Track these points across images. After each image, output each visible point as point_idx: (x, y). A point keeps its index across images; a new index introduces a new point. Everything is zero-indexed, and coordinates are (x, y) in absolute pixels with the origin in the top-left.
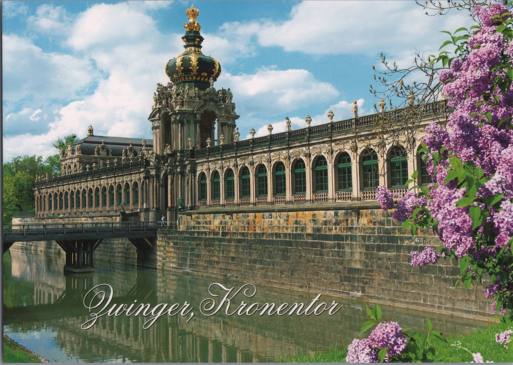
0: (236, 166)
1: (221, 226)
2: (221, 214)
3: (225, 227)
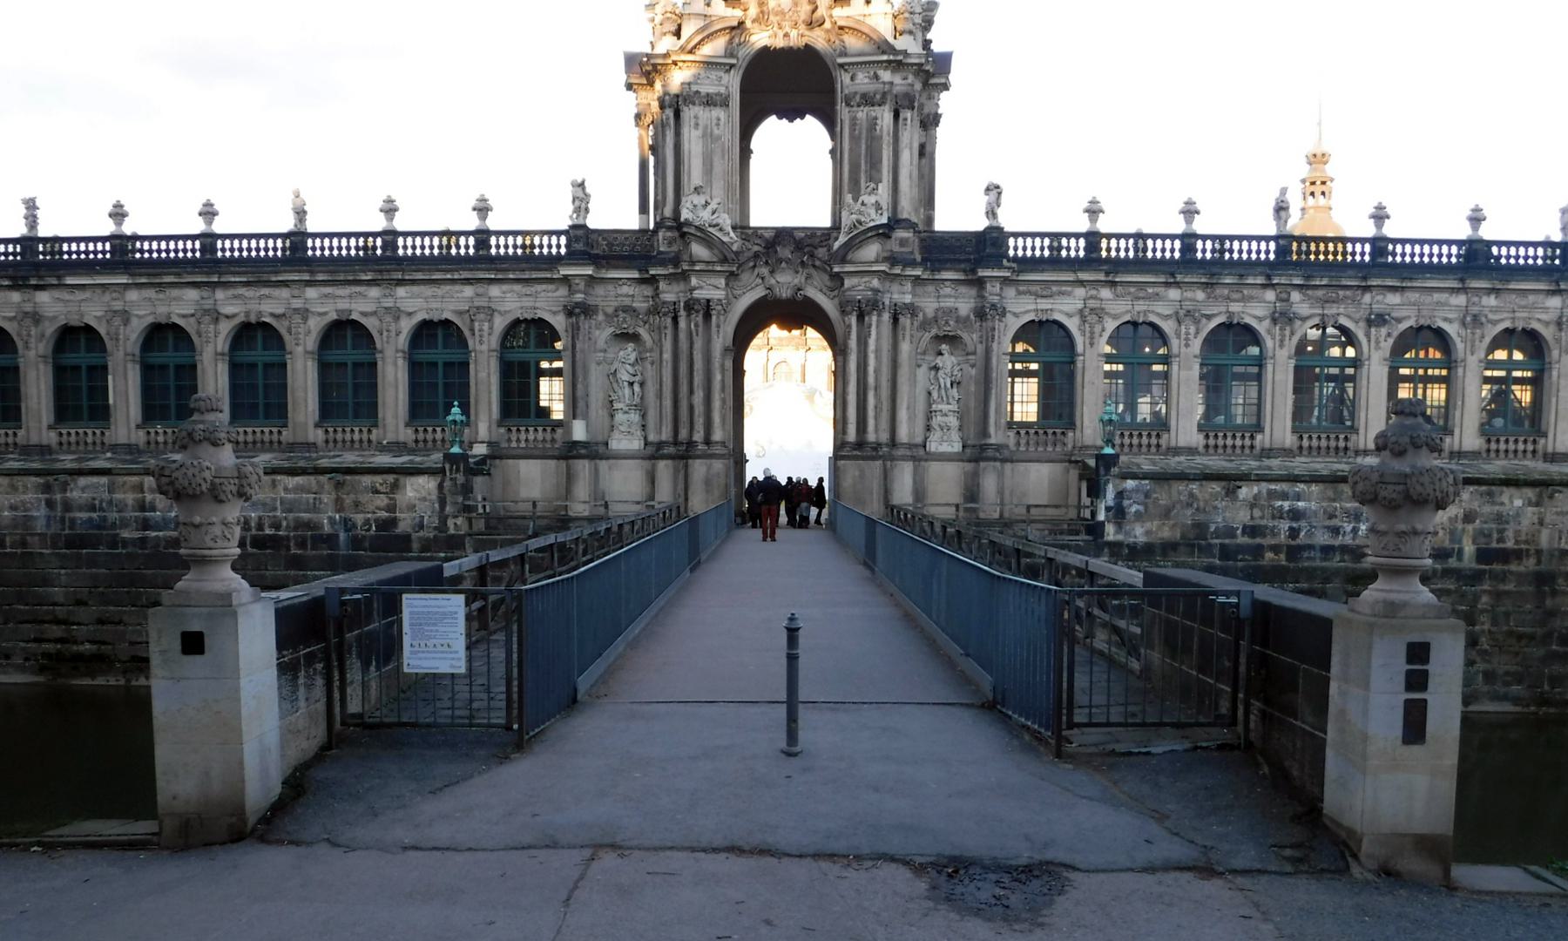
0: (1283, 318)
1: (1470, 527)
2: (1471, 488)
3: (1501, 531)
